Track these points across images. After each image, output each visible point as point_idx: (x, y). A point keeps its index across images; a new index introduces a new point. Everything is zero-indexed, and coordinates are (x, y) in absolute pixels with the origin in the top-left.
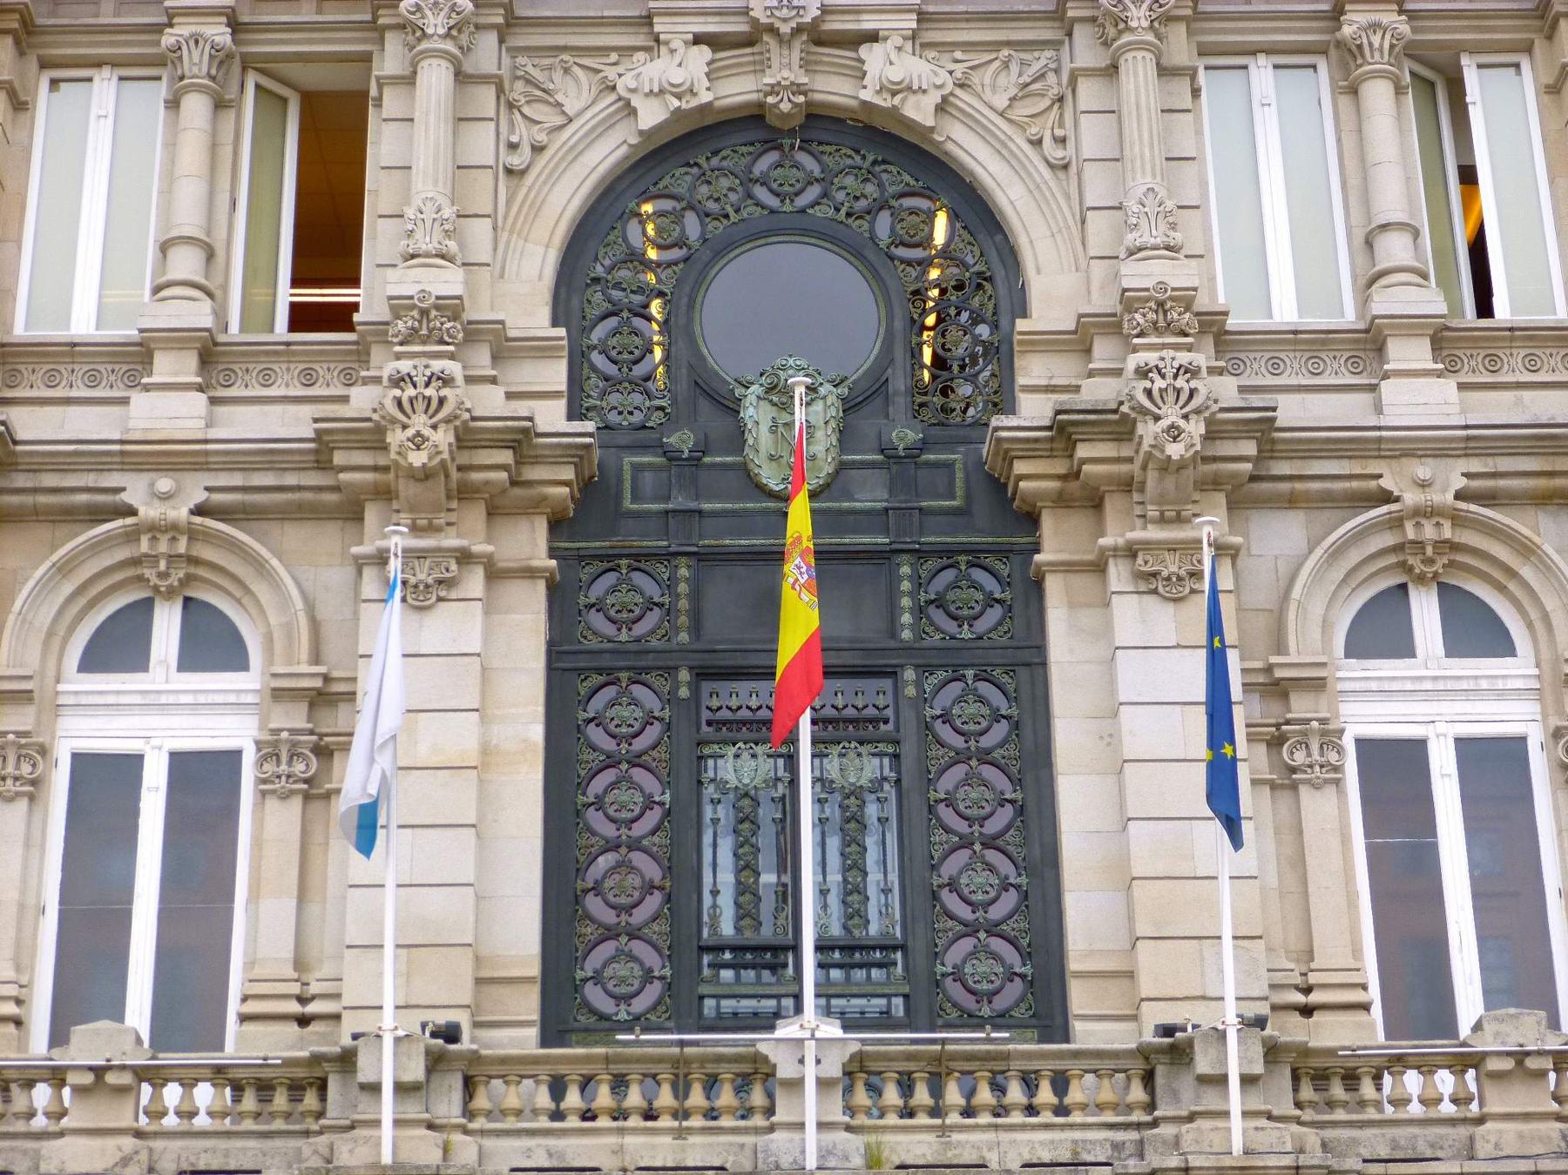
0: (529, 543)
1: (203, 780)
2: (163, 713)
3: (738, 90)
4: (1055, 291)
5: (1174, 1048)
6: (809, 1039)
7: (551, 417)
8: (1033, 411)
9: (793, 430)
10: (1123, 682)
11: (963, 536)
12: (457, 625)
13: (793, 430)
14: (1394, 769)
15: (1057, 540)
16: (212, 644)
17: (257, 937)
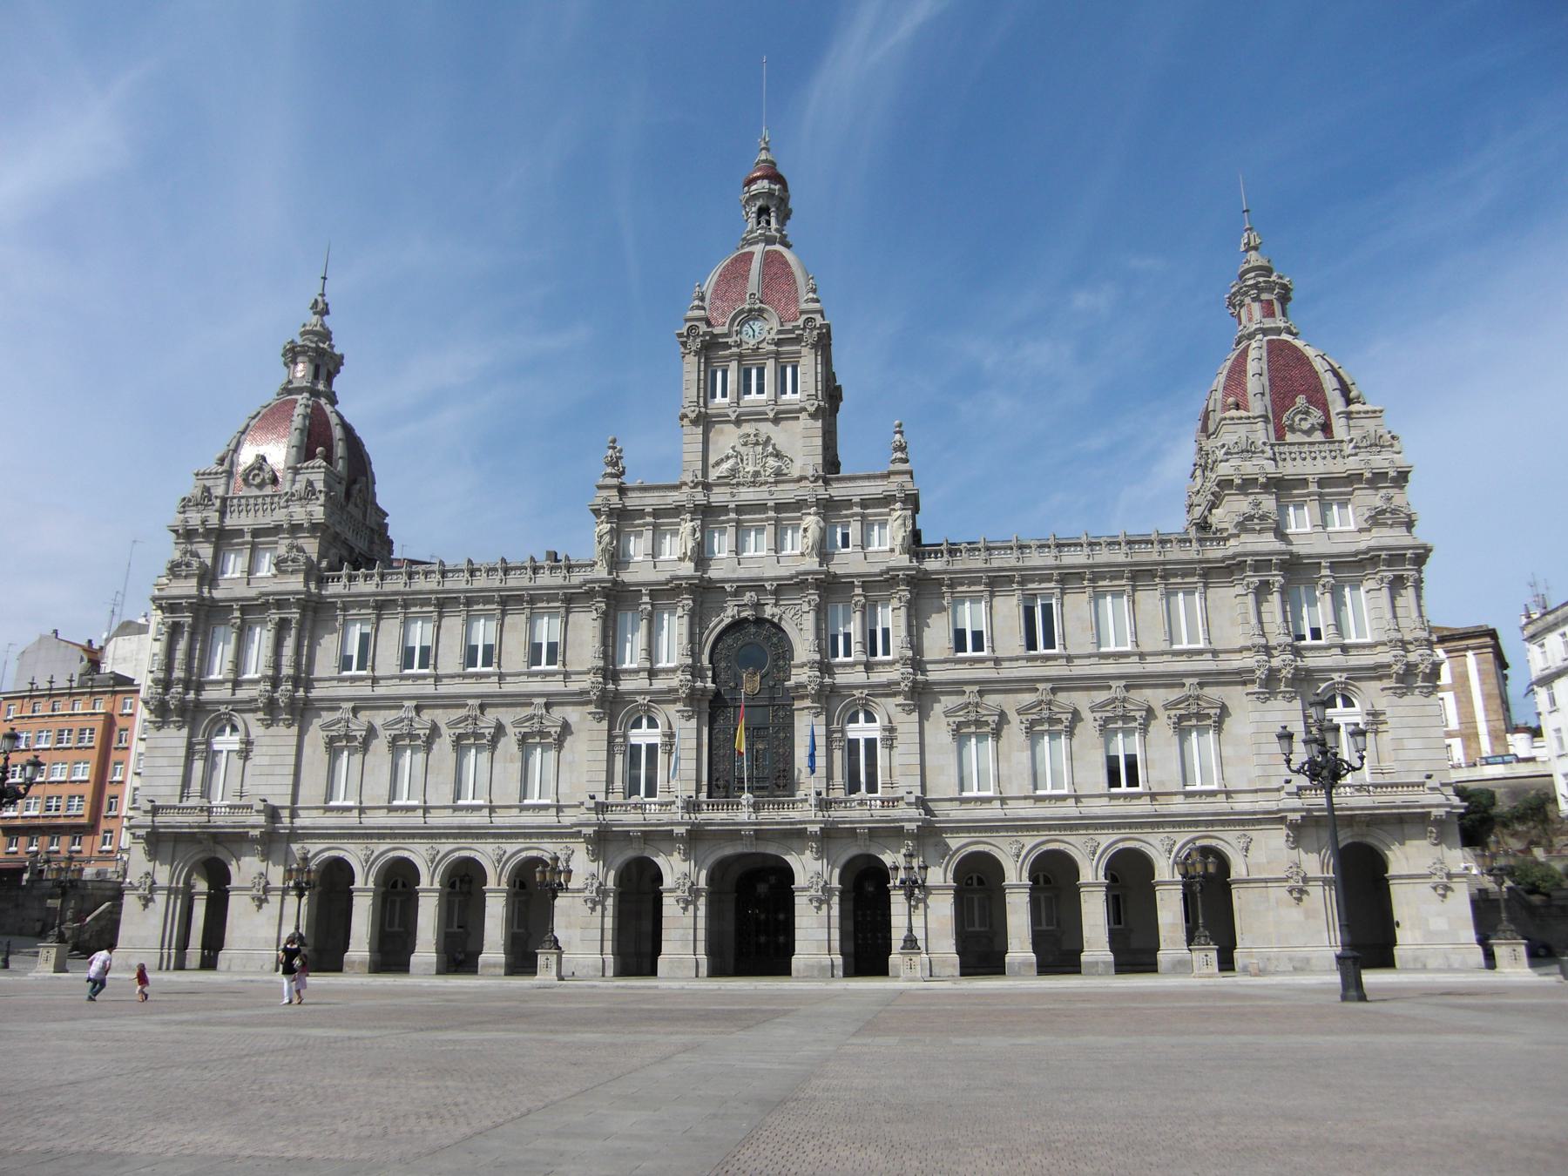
3: (744, 614)
6: (746, 797)
14: (854, 743)
16: (652, 724)
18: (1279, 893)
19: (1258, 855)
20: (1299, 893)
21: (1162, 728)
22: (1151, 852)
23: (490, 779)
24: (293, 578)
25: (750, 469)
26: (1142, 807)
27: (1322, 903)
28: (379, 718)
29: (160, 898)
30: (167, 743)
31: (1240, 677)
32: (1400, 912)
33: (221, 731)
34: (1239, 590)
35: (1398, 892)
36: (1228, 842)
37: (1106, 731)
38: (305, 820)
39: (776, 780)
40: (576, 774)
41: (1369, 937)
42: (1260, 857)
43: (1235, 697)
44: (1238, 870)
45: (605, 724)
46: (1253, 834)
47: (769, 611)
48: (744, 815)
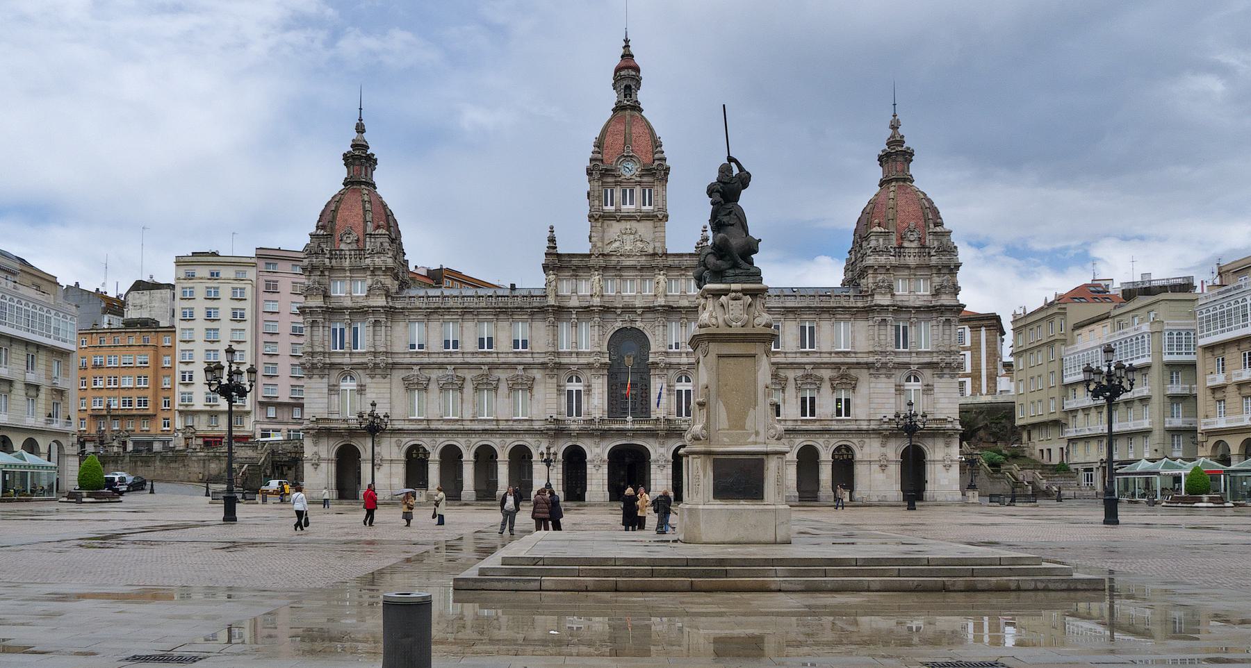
0: (606, 372)
1: (578, 392)
2: (574, 386)
4: (654, 348)
5: (658, 419)
6: (629, 418)
7: (607, 360)
8: (651, 360)
9: (629, 361)
10: (657, 385)
11: (644, 370)
12: (600, 381)
13: (629, 361)
15: (652, 372)
16: (578, 380)
17: (584, 407)
18: (875, 467)
19: (866, 449)
20: (883, 467)
21: (826, 388)
22: (817, 446)
23: (501, 407)
24: (379, 299)
25: (628, 248)
26: (816, 426)
27: (895, 470)
28: (435, 374)
29: (323, 465)
30: (317, 386)
31: (869, 366)
32: (929, 477)
33: (345, 378)
34: (871, 323)
35: (929, 467)
36: (854, 442)
37: (798, 389)
38: (398, 425)
39: (642, 407)
40: (543, 403)
41: (914, 487)
42: (868, 451)
43: (863, 374)
44: (858, 456)
45: (555, 380)
46: (867, 440)
47: (639, 325)
48: (629, 426)
